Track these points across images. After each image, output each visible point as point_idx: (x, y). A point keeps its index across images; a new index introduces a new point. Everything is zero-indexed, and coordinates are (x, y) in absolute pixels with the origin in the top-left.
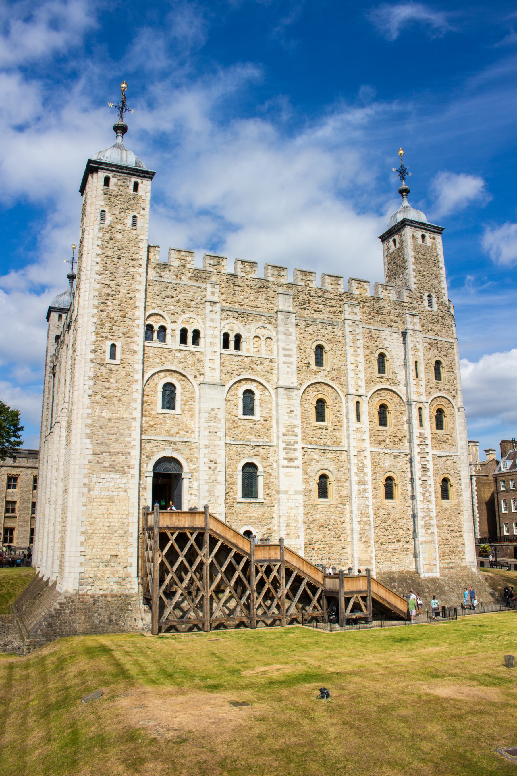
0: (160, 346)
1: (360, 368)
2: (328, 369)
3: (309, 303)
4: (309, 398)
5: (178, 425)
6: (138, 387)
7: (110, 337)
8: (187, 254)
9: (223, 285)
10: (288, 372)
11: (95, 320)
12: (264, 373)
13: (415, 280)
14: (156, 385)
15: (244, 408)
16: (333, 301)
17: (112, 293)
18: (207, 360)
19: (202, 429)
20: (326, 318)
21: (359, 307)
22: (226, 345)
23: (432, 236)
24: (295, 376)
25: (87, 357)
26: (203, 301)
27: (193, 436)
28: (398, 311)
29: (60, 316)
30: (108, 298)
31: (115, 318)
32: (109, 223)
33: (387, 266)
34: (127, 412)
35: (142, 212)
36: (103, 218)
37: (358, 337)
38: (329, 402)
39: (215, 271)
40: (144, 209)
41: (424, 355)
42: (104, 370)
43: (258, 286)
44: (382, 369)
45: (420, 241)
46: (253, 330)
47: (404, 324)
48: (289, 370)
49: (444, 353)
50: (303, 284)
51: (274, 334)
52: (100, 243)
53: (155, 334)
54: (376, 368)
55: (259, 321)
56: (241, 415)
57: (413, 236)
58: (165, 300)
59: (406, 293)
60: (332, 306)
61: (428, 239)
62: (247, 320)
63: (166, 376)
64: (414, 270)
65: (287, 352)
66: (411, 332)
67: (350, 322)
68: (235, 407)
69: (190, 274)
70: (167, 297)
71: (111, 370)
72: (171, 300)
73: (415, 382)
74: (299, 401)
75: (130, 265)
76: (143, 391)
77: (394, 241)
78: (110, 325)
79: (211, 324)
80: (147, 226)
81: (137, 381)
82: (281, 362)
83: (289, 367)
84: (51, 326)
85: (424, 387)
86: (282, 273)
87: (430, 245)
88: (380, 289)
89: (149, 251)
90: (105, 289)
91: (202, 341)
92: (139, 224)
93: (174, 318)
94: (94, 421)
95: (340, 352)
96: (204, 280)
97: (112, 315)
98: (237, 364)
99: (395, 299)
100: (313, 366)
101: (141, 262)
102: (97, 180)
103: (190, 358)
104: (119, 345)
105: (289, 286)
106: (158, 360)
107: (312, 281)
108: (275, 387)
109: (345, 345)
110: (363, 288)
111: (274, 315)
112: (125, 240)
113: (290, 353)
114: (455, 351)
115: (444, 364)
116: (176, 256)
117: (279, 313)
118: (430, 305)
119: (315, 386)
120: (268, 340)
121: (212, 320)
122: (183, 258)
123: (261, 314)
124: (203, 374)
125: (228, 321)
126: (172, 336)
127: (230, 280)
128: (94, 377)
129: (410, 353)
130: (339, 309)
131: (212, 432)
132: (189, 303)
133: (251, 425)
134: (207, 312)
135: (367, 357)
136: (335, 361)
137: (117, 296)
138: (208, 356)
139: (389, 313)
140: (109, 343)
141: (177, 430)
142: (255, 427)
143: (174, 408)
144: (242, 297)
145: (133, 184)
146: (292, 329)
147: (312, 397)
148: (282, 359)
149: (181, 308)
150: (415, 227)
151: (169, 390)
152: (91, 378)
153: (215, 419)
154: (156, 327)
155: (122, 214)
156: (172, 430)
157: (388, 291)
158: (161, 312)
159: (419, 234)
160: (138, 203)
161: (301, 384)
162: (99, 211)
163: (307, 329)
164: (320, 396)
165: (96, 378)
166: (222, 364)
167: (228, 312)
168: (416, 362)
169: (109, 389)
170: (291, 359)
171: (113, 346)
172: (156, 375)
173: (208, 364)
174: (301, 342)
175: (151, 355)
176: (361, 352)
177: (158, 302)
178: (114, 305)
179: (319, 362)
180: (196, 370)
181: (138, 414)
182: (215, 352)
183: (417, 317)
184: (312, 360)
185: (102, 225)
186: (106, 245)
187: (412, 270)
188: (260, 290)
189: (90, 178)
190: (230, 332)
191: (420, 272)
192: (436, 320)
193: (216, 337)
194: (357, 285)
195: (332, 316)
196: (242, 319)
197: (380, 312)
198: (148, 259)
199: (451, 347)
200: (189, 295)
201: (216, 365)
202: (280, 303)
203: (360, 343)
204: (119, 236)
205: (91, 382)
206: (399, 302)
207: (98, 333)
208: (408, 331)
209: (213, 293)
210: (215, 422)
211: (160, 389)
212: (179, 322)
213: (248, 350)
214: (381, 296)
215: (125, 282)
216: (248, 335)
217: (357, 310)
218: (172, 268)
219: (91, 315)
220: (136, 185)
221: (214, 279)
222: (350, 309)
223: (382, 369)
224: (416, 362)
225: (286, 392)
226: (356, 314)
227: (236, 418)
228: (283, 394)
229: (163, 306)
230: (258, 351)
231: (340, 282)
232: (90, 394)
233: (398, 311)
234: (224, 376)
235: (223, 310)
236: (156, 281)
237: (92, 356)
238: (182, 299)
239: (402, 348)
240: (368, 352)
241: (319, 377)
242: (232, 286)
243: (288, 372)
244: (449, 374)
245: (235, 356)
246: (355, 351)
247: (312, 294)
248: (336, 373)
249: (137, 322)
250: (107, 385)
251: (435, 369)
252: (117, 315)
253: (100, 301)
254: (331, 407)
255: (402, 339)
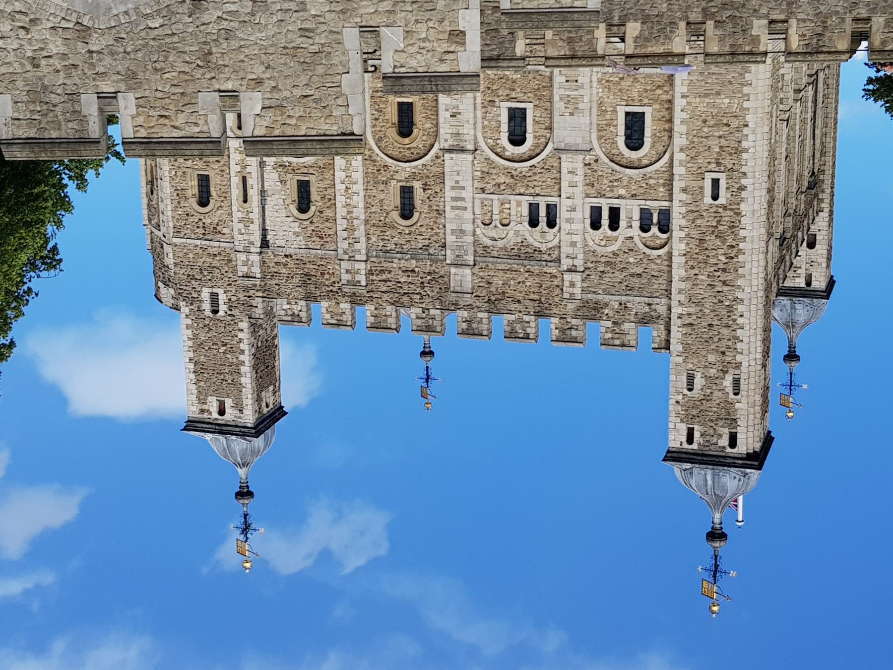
0: (648, 203)
1: (343, 187)
2: (393, 182)
3: (422, 283)
4: (424, 138)
5: (620, 90)
6: (679, 141)
7: (720, 210)
8: (611, 342)
9: (557, 299)
10: (458, 174)
11: (742, 233)
12: (494, 171)
13: (241, 335)
14: (653, 146)
15: (524, 118)
16: (384, 289)
17: (719, 274)
18: (580, 185)
19: (587, 86)
20: (395, 261)
21: (343, 282)
22: (551, 210)
23: (206, 415)
24: (447, 170)
25: (752, 180)
26: (587, 272)
27: (600, 75)
28: (274, 282)
29: (809, 284)
30: (725, 266)
31: (713, 237)
32: (727, 376)
33: (276, 364)
34: (694, 105)
35: (680, 398)
36: (736, 383)
37: (345, 234)
38: (392, 133)
39: (569, 320)
40: (677, 402)
41: (230, 214)
42: (728, 162)
43: (504, 302)
44: (304, 188)
45: (229, 403)
46: (511, 233)
47: (264, 262)
48: (457, 178)
49: (191, 219)
50: (432, 312)
51: (478, 231)
52: (739, 346)
53: (655, 220)
54: (313, 190)
55: (501, 248)
56: (529, 107)
57: (241, 411)
58: (642, 270)
59: (259, 312)
60: (385, 281)
61: (214, 407)
62: (519, 249)
63: (640, 160)
64: (242, 352)
65: (459, 204)
66: (252, 249)
67: (358, 257)
68: (537, 119)
69: (606, 311)
70: (639, 275)
71: (718, 164)
72: (634, 271)
73: (248, 169)
74: (442, 131)
75: (694, 317)
76: (670, 137)
77: (267, 406)
78: (721, 228)
79: (575, 238)
80: (672, 377)
81: (682, 150)
82: (469, 189)
83: (457, 182)
84: (824, 265)
85: (232, 163)
86: (464, 326)
87: (210, 399)
88: (303, 315)
89: (668, 341)
90: (729, 278)
91: (588, 214)
92: (684, 379)
93: (629, 244)
94: (741, 92)
95: (373, 210)
96: (585, 304)
97: (718, 242)
98: (535, 183)
99: (279, 301)
100: (417, 185)
101: (679, 322)
102: (748, 442)
103: (604, 187)
104: (708, 200)
105: (456, 306)
106: (652, 182)
107: (418, 318)
108: (478, 152)
109: (367, 222)
110: (333, 314)
111: (478, 259)
112: (704, 353)
113: (454, 204)
114: (171, 224)
115: (193, 202)
116: (628, 337)
117: (472, 263)
118: (214, 297)
119: (413, 157)
120: (488, 222)
121: (573, 244)
122: (617, 336)
123: (499, 260)
124: (586, 165)
125: (550, 245)
126: (631, 218)
127: (546, 308)
128: (741, 152)
129: (256, 215)
130: (375, 278)
131: (572, 81)
132: (608, 268)
133: (513, 95)
134: (581, 256)
135: (328, 204)
136: (382, 196)
137: (712, 269)
138: (579, 190)
139: (289, 277)
140: (722, 200)
141: (623, 83)
142: (508, 92)
143: (627, 114)
144: (528, 284)
145: (695, 440)
146: (450, 239)
147: (418, 138)
148: (467, 194)
149: (619, 259)
150: (236, 426)
151: (634, 140)
152: (746, 150)
153: (568, 100)
154: (655, 230)
155: (709, 391)
156: (630, 83)
157: (290, 312)
158: (648, 251)
159: (230, 415)
160: (686, 410)
161: (437, 157)
162: (743, 393)
163: (427, 242)
164: (407, 140)
165: (738, 151)
166: (558, 181)
167: (549, 259)
168: (245, 201)
169: (720, 137)
170: (453, 194)
171: (715, 197)
172: (653, 160)
173: (579, 179)
174: (435, 222)
175: (661, 189)
176: (341, 211)
177: (653, 266)
178: (716, 256)
179: (407, 193)
180: (596, 171)
181: (679, 103)
182: (569, 198)
183: (240, 274)
184: (419, 194)
185: (737, 372)
186: (730, 343)
187: (247, 352)
188: (499, 297)
189: (758, 446)
190: (546, 229)
191: (232, 351)
192: (205, 273)
193: (568, 221)
194: (344, 318)
195: (386, 265)
196: (530, 251)
197: (305, 278)
198: (668, 330)
199: (177, 232)
200: (607, 280)
201: (566, 178)
202: (469, 278)
203: (342, 224)
204: (712, 358)
205: (744, 144)
206: (269, 295)
207: (738, 214)
208: (258, 250)
209: (572, 285)
210: (568, 96)
211: (648, 141)
212: (621, 239)
213: (519, 204)
214: (303, 303)
215: (701, 291)
216: (519, 227)
217: (345, 277)
218: (633, 320)
219: (747, 239)
220: (690, 440)
221: (571, 306)
222: (358, 278)
223: (304, 188)
224: (245, 201)
225: (462, 144)
226: (347, 271)
227: (537, 103)
228: (466, 141)
229: (645, 261)
230: (502, 204)
231: (372, 319)
232: (746, 128)
233: (274, 282)
234: (555, 164)
235: (558, 260)
236: (656, 297)
237: (744, 181)
238: (617, 274)
239: (268, 222)
240: (328, 213)
241: (408, 169)
242: (543, 299)
243: (458, 174)
244: (183, 185)
245: (538, 195)
246: (349, 212)
247: (418, 297)
248: (380, 177)
249: (683, 234)
250: (723, 142)
251: (209, 192)
252: (712, 241)
253: (735, 260)
254: (389, 125)
255: (269, 237)
